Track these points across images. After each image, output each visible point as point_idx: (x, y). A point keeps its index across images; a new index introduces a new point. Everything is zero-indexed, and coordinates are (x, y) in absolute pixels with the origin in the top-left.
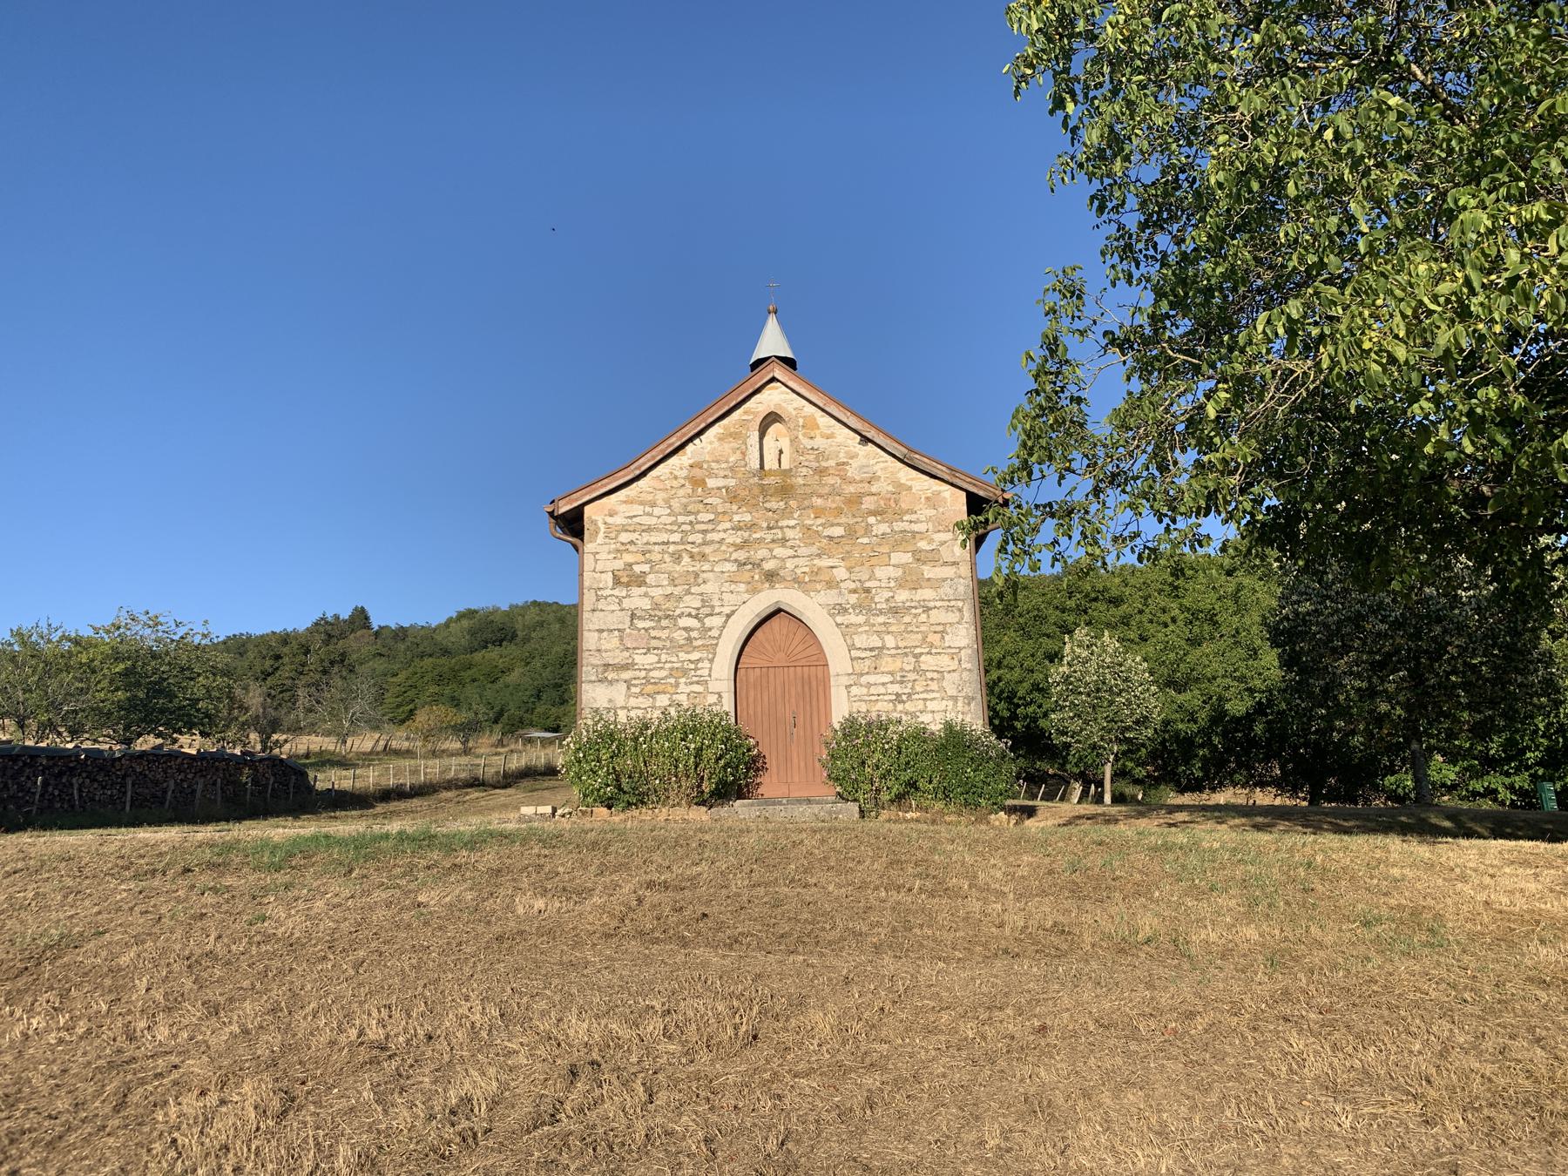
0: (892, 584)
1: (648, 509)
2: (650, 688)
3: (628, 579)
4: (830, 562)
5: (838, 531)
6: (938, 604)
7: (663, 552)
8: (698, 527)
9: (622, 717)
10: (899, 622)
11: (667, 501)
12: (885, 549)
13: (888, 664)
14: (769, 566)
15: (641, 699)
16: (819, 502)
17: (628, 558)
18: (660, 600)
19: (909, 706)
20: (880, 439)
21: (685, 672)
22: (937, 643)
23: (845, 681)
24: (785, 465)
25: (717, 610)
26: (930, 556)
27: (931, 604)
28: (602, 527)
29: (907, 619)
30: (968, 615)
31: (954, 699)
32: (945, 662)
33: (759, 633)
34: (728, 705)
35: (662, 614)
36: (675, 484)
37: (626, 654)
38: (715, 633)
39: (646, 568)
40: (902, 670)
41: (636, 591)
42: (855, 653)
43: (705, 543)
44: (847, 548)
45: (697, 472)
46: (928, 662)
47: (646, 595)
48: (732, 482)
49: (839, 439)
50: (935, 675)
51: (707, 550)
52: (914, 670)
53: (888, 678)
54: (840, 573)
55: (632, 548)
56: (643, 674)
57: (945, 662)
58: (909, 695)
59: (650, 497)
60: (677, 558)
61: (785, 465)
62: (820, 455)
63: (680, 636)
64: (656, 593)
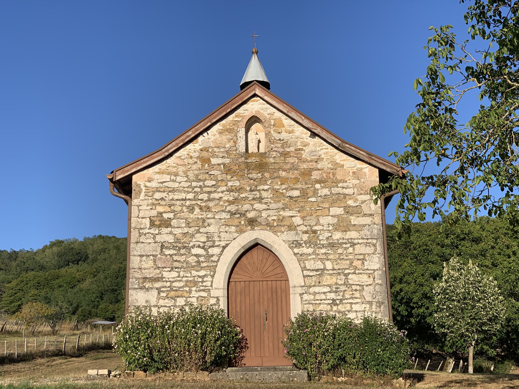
0: (331, 228)
1: (173, 177)
2: (172, 294)
3: (160, 223)
4: (290, 213)
5: (296, 193)
6: (360, 241)
7: (182, 205)
8: (205, 189)
9: (155, 312)
10: (335, 253)
11: (185, 172)
12: (326, 205)
13: (328, 280)
14: (250, 215)
15: (167, 301)
16: (284, 174)
17: (160, 209)
18: (179, 236)
19: (341, 308)
20: (324, 134)
21: (195, 283)
22: (359, 267)
23: (300, 290)
24: (262, 150)
25: (217, 243)
26: (355, 209)
27: (356, 241)
28: (144, 189)
29: (340, 251)
30: (379, 249)
31: (370, 303)
32: (364, 279)
33: (244, 259)
34: (223, 305)
35: (181, 246)
36: (191, 161)
37: (158, 271)
38: (215, 258)
39: (171, 215)
40: (336, 284)
41: (164, 230)
42: (306, 273)
43: (209, 200)
44: (302, 204)
45: (205, 154)
46: (353, 279)
47: (171, 233)
48: (227, 161)
49: (297, 134)
50: (358, 288)
51: (211, 204)
52: (344, 284)
53: (327, 289)
54: (297, 220)
55: (162, 203)
56: (168, 284)
57: (364, 279)
58: (341, 300)
59: (174, 170)
60: (191, 209)
61: (262, 150)
62: (285, 144)
63: (192, 260)
64: (177, 231)
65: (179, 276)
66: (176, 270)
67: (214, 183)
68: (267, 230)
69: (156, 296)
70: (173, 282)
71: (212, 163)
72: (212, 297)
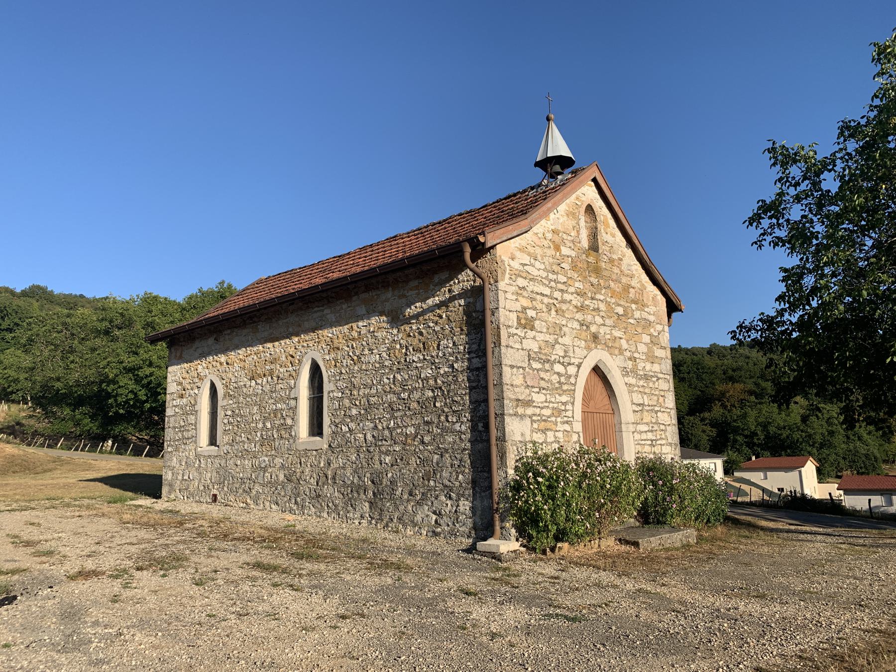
3: (527, 324)
23: (632, 428)
37: (527, 391)
66: (544, 391)
67: (565, 280)
70: (542, 408)
71: (563, 253)
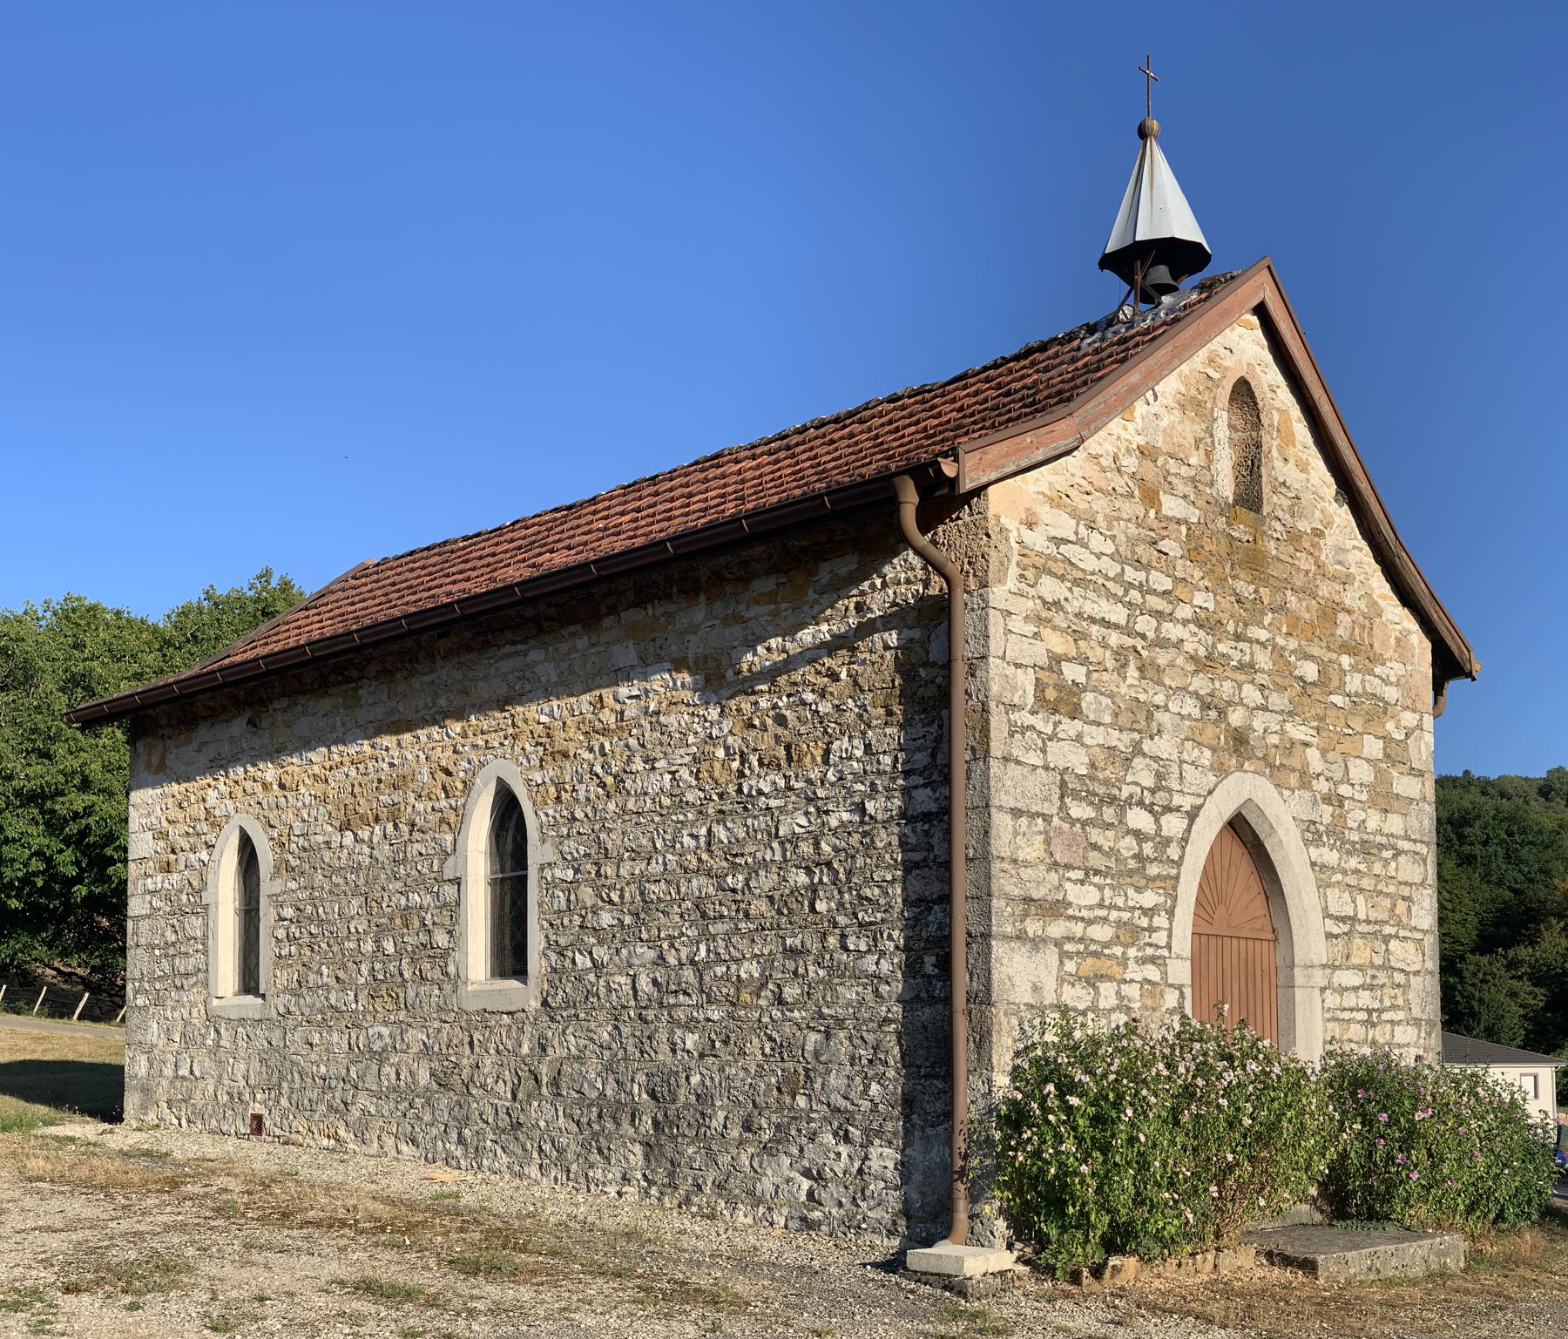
23: (1319, 978)
37: (1053, 877)
65: (1101, 905)
66: (1096, 879)
67: (1167, 584)
68: (1263, 774)
69: (1055, 972)
70: (1090, 922)
71: (1166, 511)
72: (1171, 986)
